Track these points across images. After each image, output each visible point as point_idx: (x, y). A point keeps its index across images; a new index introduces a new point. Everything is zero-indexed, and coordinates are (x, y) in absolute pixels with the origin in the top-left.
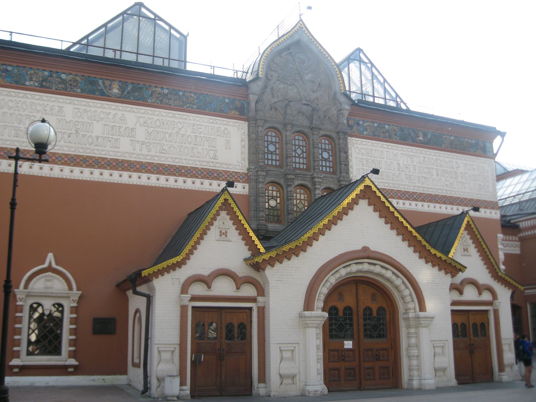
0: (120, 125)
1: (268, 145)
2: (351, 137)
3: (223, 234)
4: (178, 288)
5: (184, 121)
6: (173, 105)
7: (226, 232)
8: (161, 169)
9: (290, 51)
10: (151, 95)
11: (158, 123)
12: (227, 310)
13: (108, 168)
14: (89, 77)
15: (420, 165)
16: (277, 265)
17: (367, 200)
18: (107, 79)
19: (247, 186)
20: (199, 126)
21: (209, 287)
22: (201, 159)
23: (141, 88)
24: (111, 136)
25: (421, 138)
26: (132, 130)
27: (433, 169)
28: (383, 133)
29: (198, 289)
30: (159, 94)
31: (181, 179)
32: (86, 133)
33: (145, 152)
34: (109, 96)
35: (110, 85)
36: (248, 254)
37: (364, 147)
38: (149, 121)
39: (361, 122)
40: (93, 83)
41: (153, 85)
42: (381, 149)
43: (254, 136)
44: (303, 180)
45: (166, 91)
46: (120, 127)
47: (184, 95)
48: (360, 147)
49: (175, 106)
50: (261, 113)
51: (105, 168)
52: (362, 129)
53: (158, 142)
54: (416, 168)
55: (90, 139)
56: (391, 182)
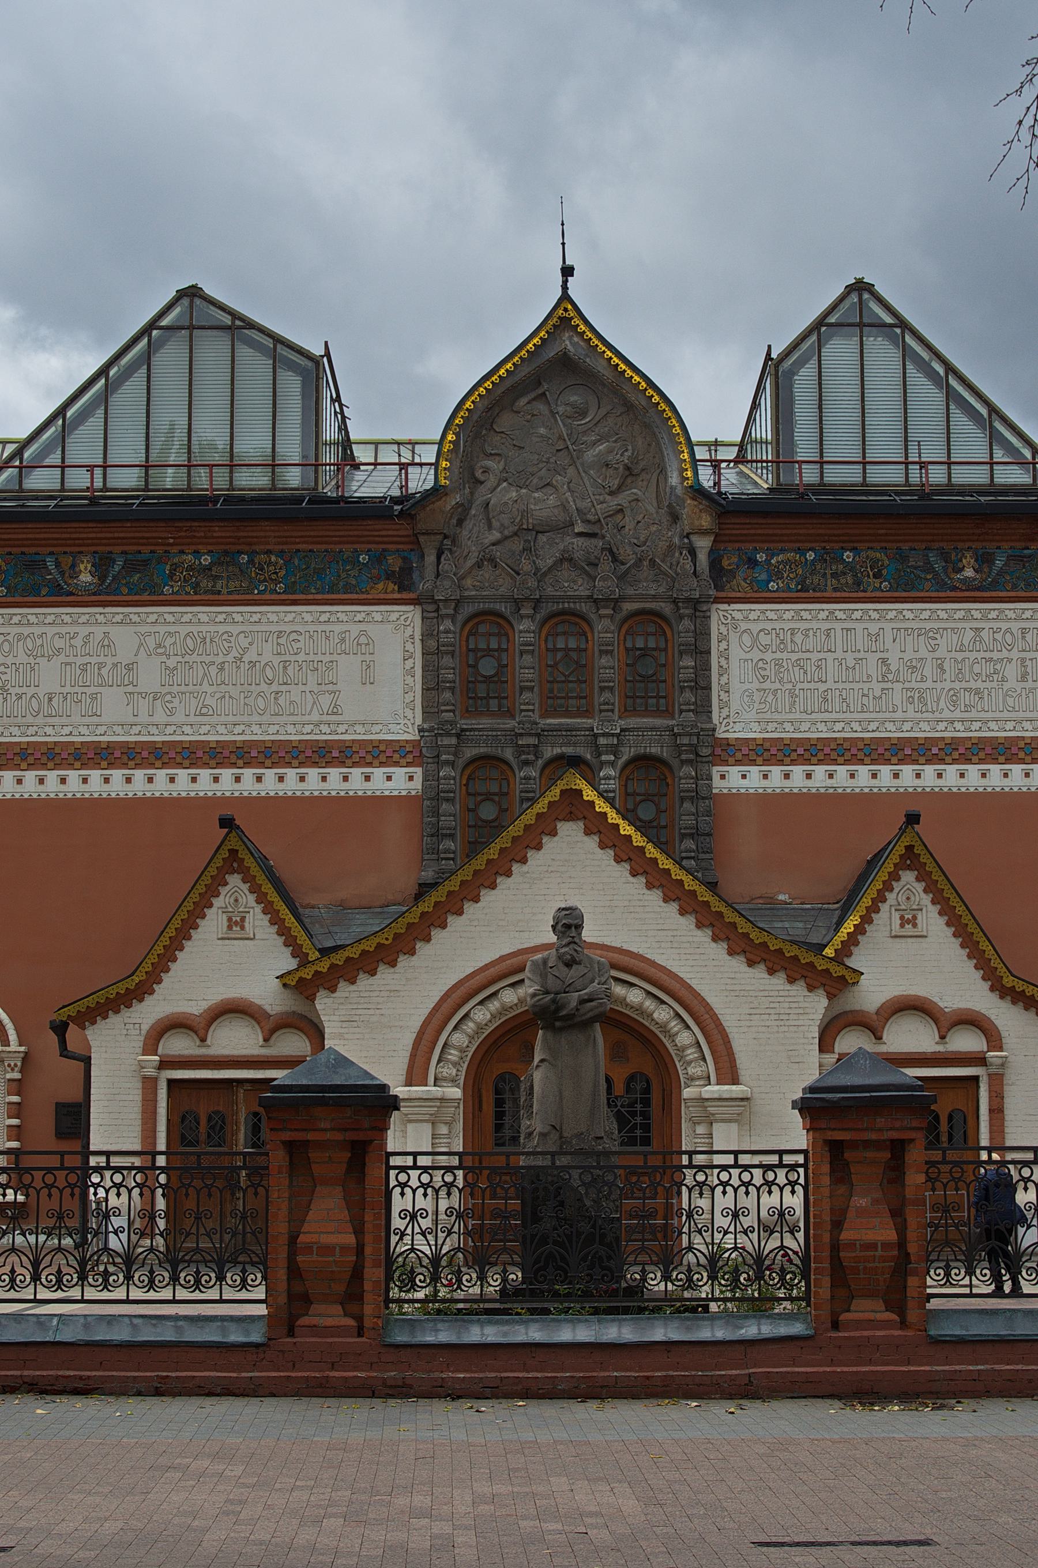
0: (102, 659)
1: (477, 660)
2: (729, 603)
3: (236, 924)
4: (138, 1044)
5: (256, 628)
6: (225, 591)
7: (243, 919)
8: (200, 754)
9: (540, 391)
10: (171, 576)
11: (189, 641)
12: (248, 1086)
13: (78, 764)
14: (23, 553)
15: (960, 656)
16: (344, 989)
17: (581, 824)
18: (65, 553)
19: (418, 772)
20: (294, 636)
21: (203, 1040)
22: (298, 719)
23: (146, 563)
24: (80, 690)
25: (969, 573)
26: (130, 667)
27: (1010, 660)
28: (834, 575)
29: (179, 1045)
30: (191, 568)
31: (248, 774)
32: (24, 689)
33: (160, 717)
34: (71, 594)
35: (73, 566)
36: (292, 964)
37: (769, 626)
38: (169, 641)
39: (761, 557)
40: (34, 565)
41: (175, 550)
42: (827, 625)
43: (432, 644)
44: (568, 744)
45: (206, 560)
46: (101, 666)
47: (251, 561)
48: (755, 628)
49: (230, 593)
50: (447, 583)
51: (71, 766)
52: (764, 576)
53: (191, 688)
54: (946, 666)
55: (34, 703)
56: (856, 716)
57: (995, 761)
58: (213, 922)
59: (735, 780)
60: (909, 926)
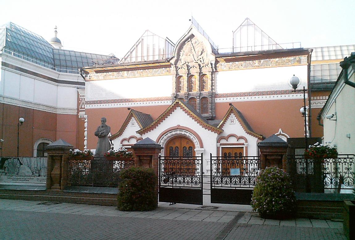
28: (235, 66)
29: (126, 143)
57: (261, 95)
58: (130, 124)
59: (218, 100)
60: (232, 122)
